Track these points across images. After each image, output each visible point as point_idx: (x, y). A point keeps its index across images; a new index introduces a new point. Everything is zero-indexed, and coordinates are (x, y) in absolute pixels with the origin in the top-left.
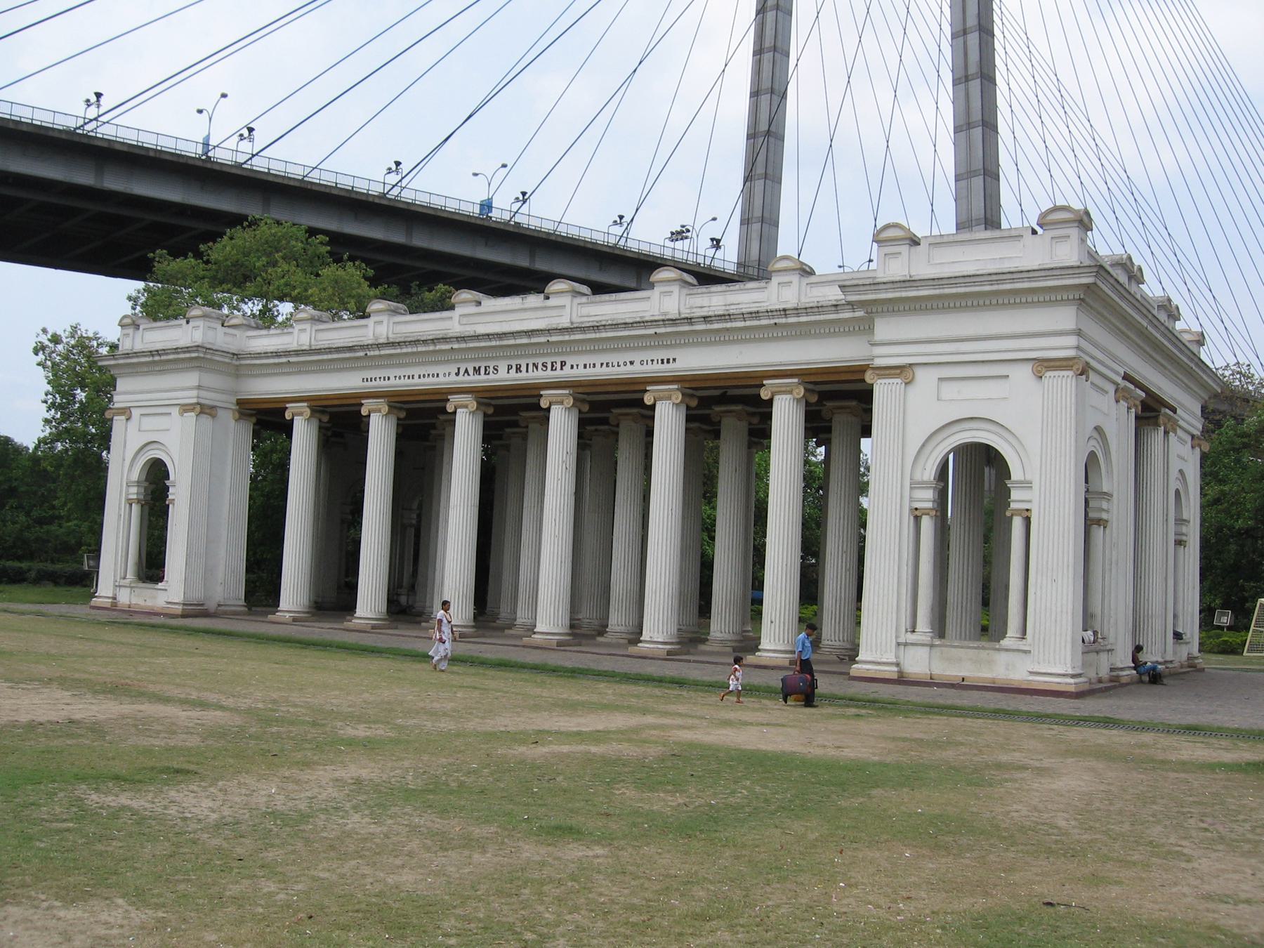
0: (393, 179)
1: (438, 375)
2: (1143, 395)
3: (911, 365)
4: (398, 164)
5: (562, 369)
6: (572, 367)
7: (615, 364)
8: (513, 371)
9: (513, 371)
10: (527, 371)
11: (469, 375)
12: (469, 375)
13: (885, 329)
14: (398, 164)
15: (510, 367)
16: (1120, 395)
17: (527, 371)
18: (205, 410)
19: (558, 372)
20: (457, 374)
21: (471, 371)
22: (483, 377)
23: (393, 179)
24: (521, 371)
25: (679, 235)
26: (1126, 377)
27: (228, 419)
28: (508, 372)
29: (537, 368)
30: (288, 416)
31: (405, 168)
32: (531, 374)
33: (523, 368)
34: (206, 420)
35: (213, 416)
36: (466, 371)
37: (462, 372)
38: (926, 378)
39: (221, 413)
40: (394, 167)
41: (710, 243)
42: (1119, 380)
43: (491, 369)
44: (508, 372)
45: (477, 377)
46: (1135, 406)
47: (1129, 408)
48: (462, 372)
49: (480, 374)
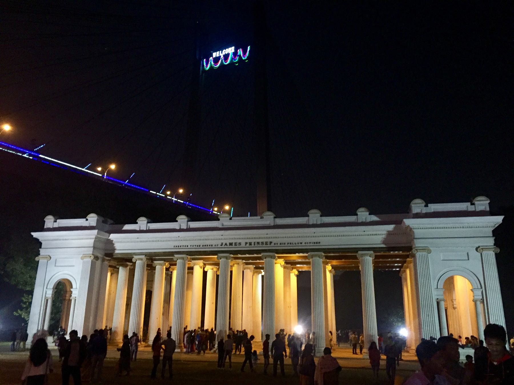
1: (212, 245)
5: (270, 244)
6: (275, 244)
7: (294, 243)
8: (248, 245)
9: (248, 245)
10: (254, 245)
11: (227, 245)
12: (227, 245)
15: (246, 243)
17: (254, 245)
19: (269, 245)
20: (221, 245)
21: (228, 244)
24: (251, 245)
28: (246, 245)
29: (259, 244)
30: (134, 260)
32: (256, 245)
33: (253, 244)
36: (226, 244)
37: (224, 244)
43: (238, 244)
44: (246, 245)
45: (230, 246)
48: (224, 244)
49: (232, 245)
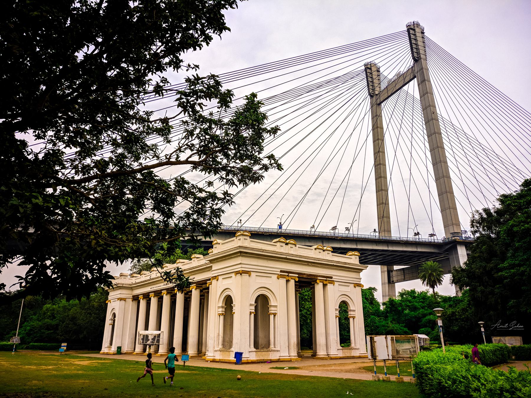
0: (240, 225)
2: (297, 275)
3: (218, 276)
4: (241, 220)
13: (215, 266)
14: (241, 220)
16: (280, 277)
18: (121, 299)
22: (167, 286)
23: (240, 225)
25: (334, 228)
26: (281, 271)
27: (130, 301)
31: (243, 222)
34: (123, 302)
35: (125, 300)
38: (220, 278)
39: (127, 300)
40: (239, 221)
41: (345, 229)
42: (279, 273)
46: (295, 279)
47: (288, 281)
